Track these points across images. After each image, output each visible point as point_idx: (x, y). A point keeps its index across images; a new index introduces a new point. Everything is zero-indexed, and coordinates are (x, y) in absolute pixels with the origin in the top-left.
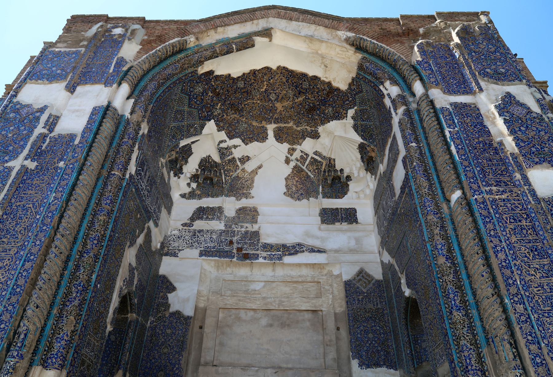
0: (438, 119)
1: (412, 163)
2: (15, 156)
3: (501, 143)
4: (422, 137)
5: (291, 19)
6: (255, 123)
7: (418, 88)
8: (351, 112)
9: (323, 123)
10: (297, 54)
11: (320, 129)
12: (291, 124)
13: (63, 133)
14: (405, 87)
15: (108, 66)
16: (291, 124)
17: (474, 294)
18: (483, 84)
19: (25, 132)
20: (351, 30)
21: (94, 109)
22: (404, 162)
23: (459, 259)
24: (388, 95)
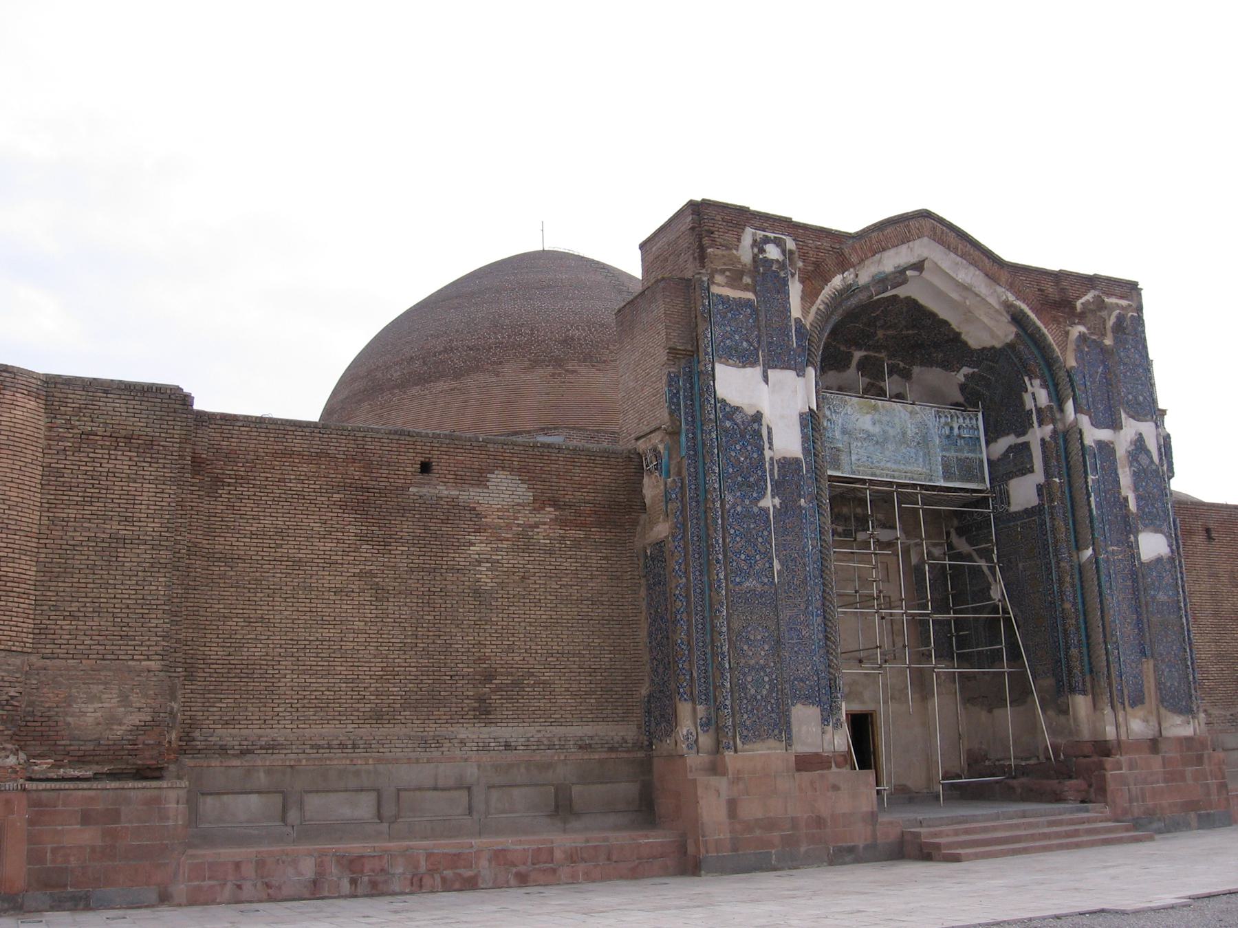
0: (1084, 458)
1: (1052, 501)
2: (762, 495)
3: (1126, 499)
4: (1064, 470)
5: (949, 248)
6: (843, 348)
7: (1069, 406)
8: (966, 370)
9: (922, 364)
10: (939, 295)
11: (916, 370)
12: (883, 355)
13: (788, 456)
14: (1053, 394)
15: (790, 339)
16: (883, 355)
17: (1088, 637)
18: (1123, 416)
19: (755, 455)
20: (1011, 287)
21: (801, 415)
22: (1040, 488)
23: (1080, 606)
24: (1033, 394)
